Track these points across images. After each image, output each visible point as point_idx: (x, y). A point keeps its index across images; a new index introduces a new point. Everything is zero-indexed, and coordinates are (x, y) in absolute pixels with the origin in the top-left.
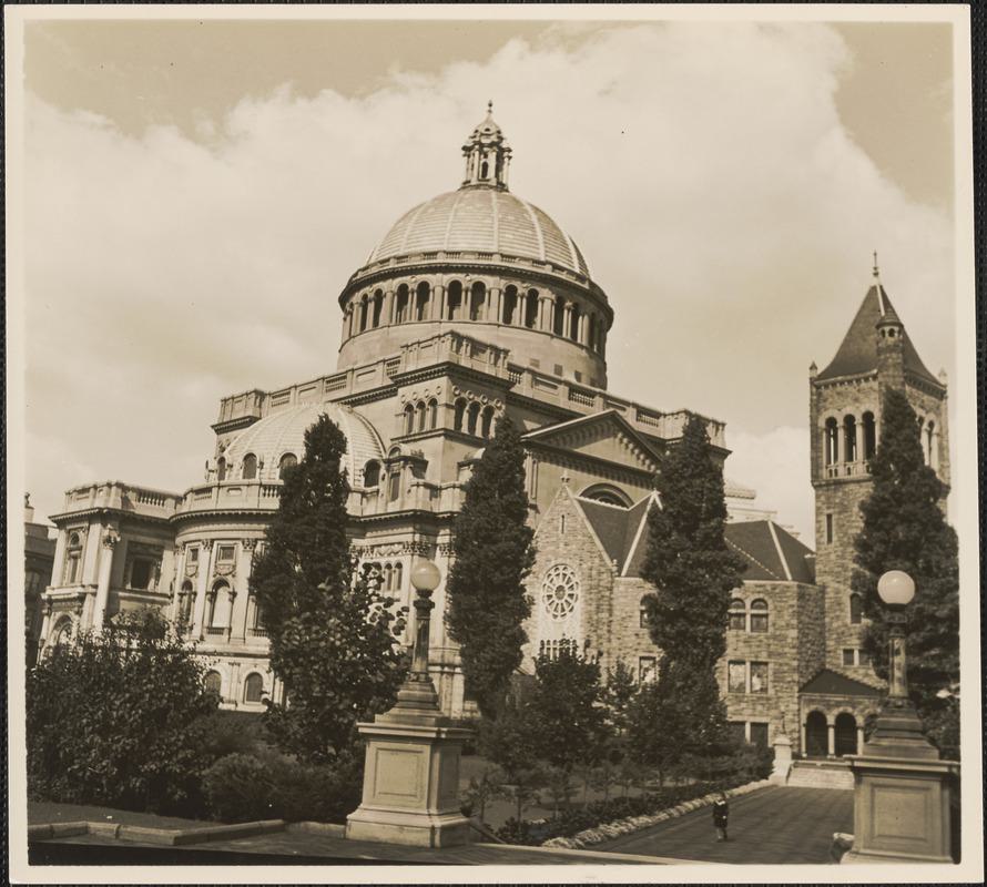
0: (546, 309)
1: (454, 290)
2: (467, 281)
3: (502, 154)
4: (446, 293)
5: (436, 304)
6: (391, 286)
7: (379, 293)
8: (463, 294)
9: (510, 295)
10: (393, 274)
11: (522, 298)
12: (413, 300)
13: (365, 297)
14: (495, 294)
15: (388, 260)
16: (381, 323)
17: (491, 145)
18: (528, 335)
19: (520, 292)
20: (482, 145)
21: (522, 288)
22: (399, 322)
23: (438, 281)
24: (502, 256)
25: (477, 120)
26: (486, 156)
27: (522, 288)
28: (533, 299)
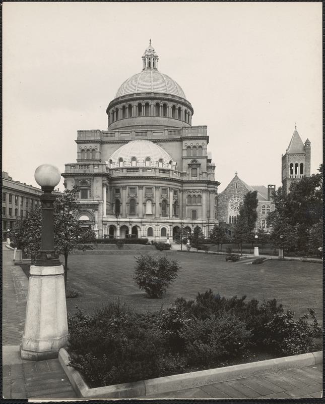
0: (169, 110)
1: (140, 106)
2: (143, 104)
3: (156, 58)
6: (120, 106)
7: (117, 108)
9: (157, 105)
10: (121, 102)
11: (161, 106)
12: (127, 111)
14: (152, 106)
15: (118, 98)
16: (119, 118)
17: (151, 55)
18: (164, 119)
19: (160, 105)
20: (148, 56)
21: (161, 104)
22: (124, 118)
24: (154, 93)
25: (146, 46)
26: (150, 59)
28: (165, 106)
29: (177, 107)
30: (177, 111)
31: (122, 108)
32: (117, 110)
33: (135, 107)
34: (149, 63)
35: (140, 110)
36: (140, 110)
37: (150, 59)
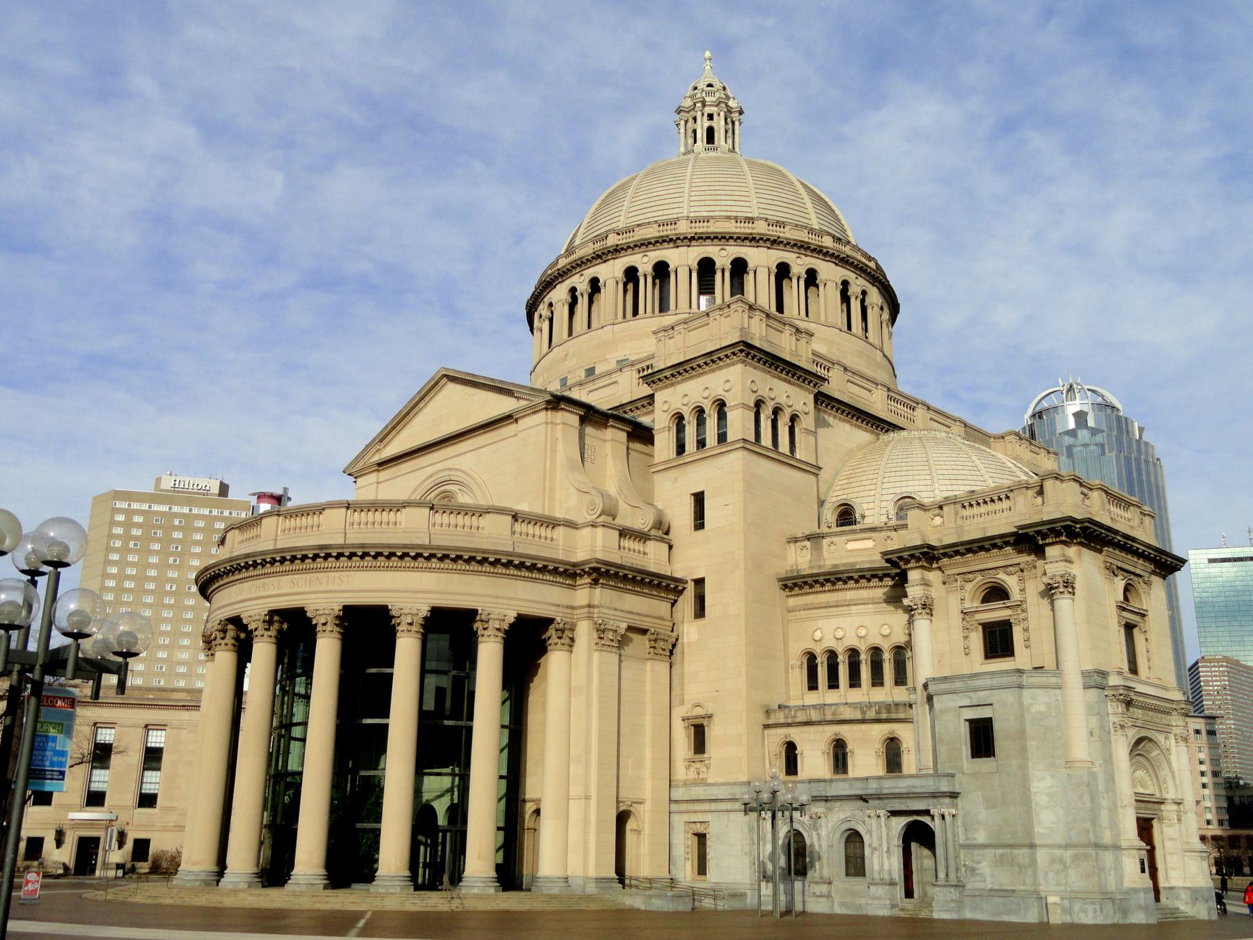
1: (706, 268)
2: (723, 257)
4: (695, 275)
5: (683, 285)
8: (718, 276)
9: (783, 271)
10: (617, 251)
11: (799, 279)
13: (573, 290)
21: (799, 265)
23: (683, 260)
26: (711, 117)
27: (799, 265)
29: (854, 290)
30: (855, 306)
31: (620, 274)
32: (595, 285)
33: (683, 275)
34: (710, 133)
35: (706, 286)
36: (706, 286)
37: (711, 117)
